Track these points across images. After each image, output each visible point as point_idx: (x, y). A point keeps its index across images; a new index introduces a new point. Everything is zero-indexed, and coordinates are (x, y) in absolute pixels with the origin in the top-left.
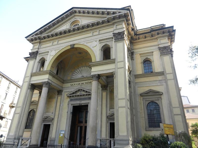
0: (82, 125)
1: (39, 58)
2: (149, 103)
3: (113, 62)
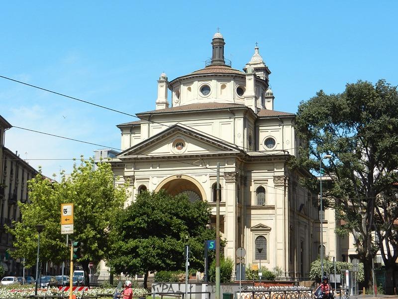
2: (257, 238)
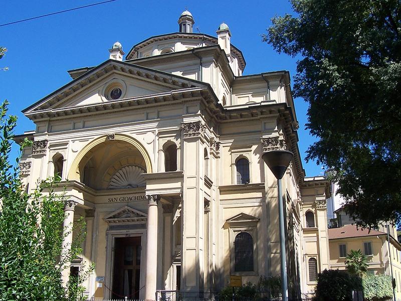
0: (130, 267)
1: (50, 154)
3: (180, 177)
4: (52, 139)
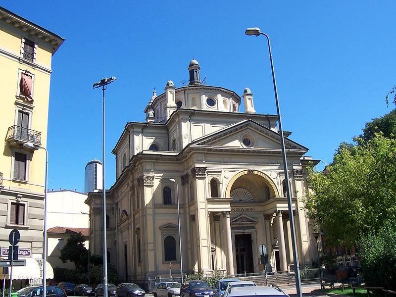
4: (210, 167)
